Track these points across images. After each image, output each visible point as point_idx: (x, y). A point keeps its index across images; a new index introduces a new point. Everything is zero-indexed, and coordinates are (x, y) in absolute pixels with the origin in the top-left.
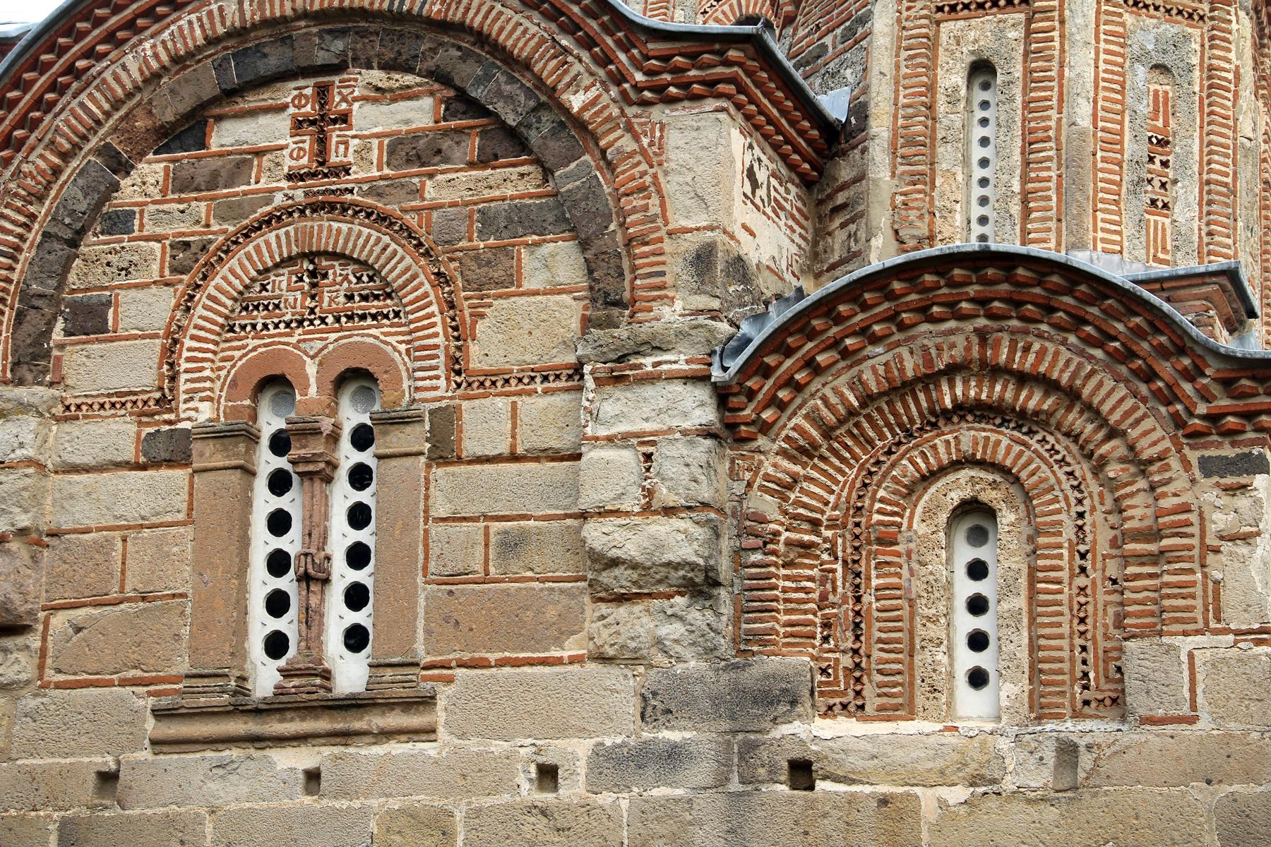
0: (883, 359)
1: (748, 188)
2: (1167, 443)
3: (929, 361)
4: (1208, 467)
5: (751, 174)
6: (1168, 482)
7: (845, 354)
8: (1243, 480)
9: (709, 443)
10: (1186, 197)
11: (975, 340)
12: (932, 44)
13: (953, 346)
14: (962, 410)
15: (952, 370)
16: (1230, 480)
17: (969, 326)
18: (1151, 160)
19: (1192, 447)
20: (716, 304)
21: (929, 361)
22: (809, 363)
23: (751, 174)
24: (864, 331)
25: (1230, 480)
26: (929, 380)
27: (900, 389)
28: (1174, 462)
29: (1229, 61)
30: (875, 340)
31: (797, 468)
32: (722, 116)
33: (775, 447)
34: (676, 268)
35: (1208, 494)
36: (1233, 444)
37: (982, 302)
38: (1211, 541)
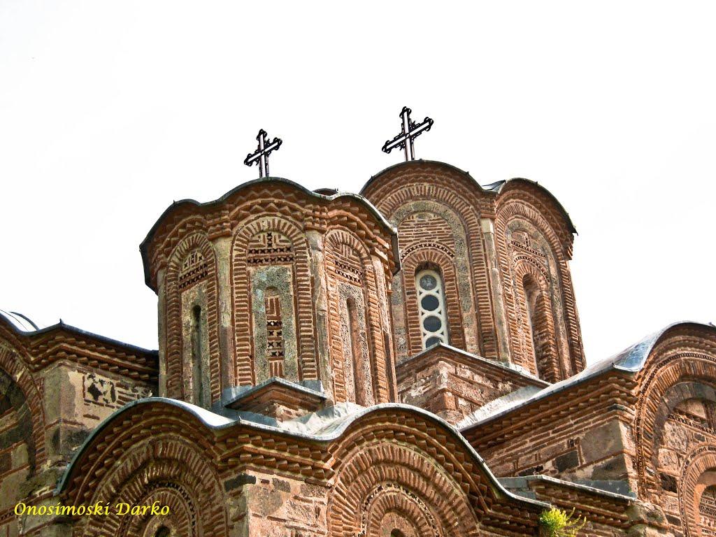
0: (121, 466)
1: (89, 397)
2: (213, 479)
3: (136, 463)
4: (229, 486)
5: (93, 390)
6: (214, 498)
7: (109, 467)
8: (239, 489)
9: (56, 527)
10: (291, 348)
11: (151, 447)
12: (178, 305)
13: (143, 452)
14: (156, 483)
15: (145, 464)
16: (235, 490)
17: (147, 441)
18: (271, 333)
19: (222, 478)
20: (60, 458)
21: (136, 463)
22: (93, 477)
23: (93, 390)
24: (110, 454)
25: (235, 490)
26: (139, 470)
27: (128, 479)
28: (216, 487)
29: (306, 276)
30: (117, 457)
31: (97, 529)
32: (63, 368)
33: (88, 521)
34: (48, 445)
35: (229, 501)
36: (236, 472)
37: (148, 427)
38: (230, 523)
